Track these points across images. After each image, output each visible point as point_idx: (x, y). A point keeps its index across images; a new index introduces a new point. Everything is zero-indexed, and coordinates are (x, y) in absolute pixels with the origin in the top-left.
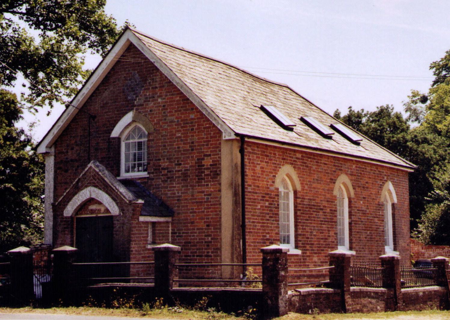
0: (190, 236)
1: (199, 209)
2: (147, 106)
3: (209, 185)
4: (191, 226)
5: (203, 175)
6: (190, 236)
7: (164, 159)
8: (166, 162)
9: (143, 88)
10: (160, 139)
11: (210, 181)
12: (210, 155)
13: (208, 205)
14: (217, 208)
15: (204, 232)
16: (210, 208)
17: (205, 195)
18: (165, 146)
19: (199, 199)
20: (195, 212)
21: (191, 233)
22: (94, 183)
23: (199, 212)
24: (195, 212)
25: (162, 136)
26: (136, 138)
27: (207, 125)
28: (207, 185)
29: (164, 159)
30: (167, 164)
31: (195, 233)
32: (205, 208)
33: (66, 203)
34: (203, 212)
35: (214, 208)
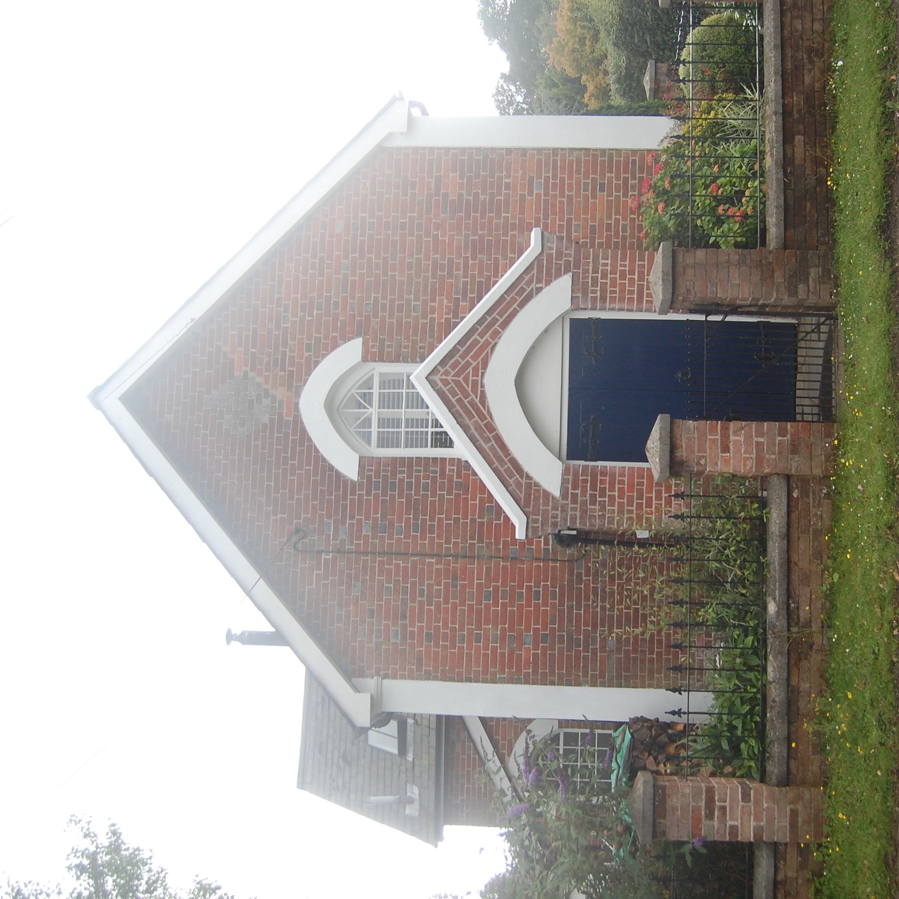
0: (625, 238)
1: (562, 210)
2: (297, 360)
3: (507, 181)
4: (601, 237)
5: (482, 197)
6: (625, 238)
7: (433, 310)
8: (441, 301)
9: (251, 374)
10: (383, 320)
11: (500, 178)
12: (438, 179)
13: (554, 185)
14: (563, 160)
15: (618, 197)
16: (562, 180)
17: (531, 193)
18: (400, 307)
19: (538, 211)
20: (569, 221)
21: (617, 234)
22: (476, 369)
23: (570, 213)
24: (569, 221)
25: (376, 316)
26: (371, 410)
27: (368, 185)
28: (508, 186)
29: (433, 310)
30: (445, 301)
31: (617, 221)
32: (562, 195)
33: (523, 481)
34: (570, 198)
35: (563, 169)
